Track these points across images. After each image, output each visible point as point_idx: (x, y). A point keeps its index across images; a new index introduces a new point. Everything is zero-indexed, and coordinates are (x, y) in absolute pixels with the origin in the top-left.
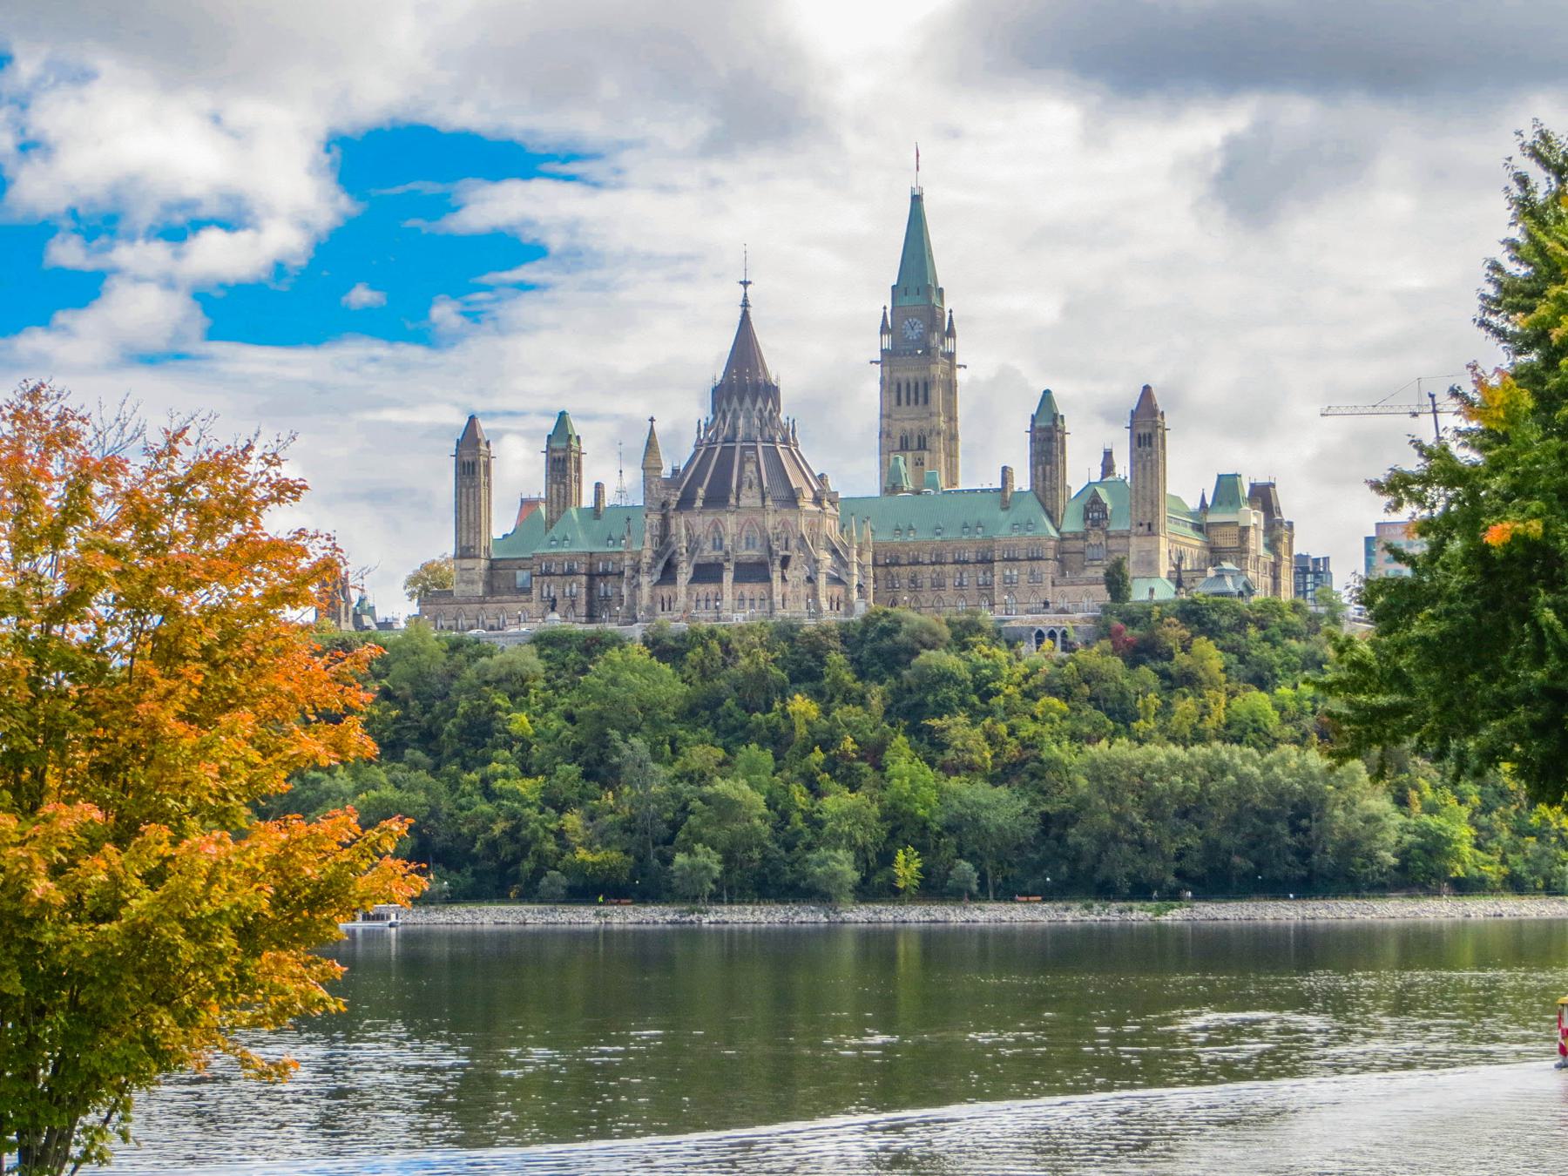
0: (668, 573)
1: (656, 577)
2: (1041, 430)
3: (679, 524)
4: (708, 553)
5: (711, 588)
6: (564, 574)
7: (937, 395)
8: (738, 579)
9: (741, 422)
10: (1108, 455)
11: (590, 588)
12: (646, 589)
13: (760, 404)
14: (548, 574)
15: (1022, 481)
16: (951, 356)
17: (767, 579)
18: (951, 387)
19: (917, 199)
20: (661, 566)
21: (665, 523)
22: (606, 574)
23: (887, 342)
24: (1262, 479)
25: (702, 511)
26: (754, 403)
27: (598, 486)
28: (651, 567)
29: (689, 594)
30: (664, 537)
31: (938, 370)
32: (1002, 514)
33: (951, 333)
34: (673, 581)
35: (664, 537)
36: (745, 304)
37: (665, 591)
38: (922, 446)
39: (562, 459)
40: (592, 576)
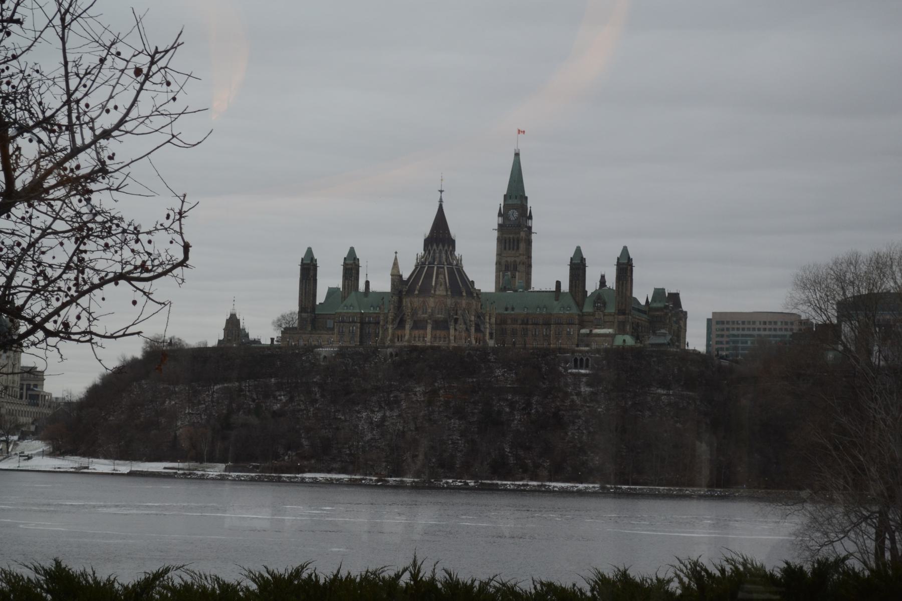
0: (401, 324)
1: (395, 326)
2: (575, 264)
3: (406, 301)
4: (421, 315)
5: (421, 332)
6: (350, 322)
7: (522, 246)
8: (433, 328)
10: (603, 277)
11: (361, 329)
12: (390, 331)
13: (446, 248)
14: (343, 322)
15: (565, 287)
16: (530, 228)
17: (448, 329)
18: (529, 243)
19: (517, 155)
20: (398, 320)
21: (400, 301)
22: (369, 323)
23: (501, 220)
24: (673, 291)
25: (418, 296)
26: (444, 247)
27: (367, 283)
28: (393, 320)
29: (410, 334)
30: (399, 306)
31: (523, 234)
32: (556, 303)
33: (530, 217)
34: (404, 328)
35: (399, 306)
36: (441, 201)
37: (399, 332)
38: (515, 269)
39: (351, 268)
40: (362, 323)
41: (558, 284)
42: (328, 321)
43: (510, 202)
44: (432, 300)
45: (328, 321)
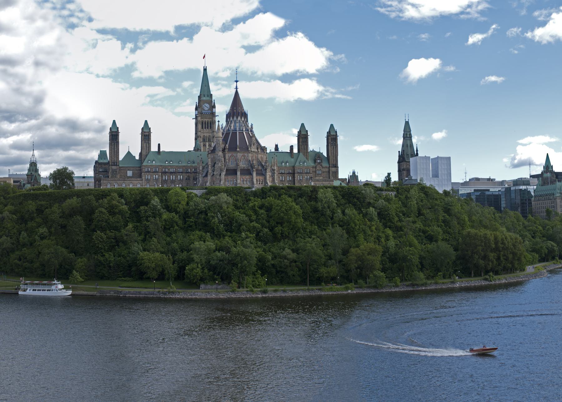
5: (248, 177)
9: (238, 125)
11: (162, 177)
15: (295, 151)
22: (165, 173)
25: (238, 152)
32: (292, 160)
36: (237, 88)
39: (146, 135)
41: (292, 147)
42: (128, 172)
43: (204, 98)
44: (250, 155)
45: (128, 172)
